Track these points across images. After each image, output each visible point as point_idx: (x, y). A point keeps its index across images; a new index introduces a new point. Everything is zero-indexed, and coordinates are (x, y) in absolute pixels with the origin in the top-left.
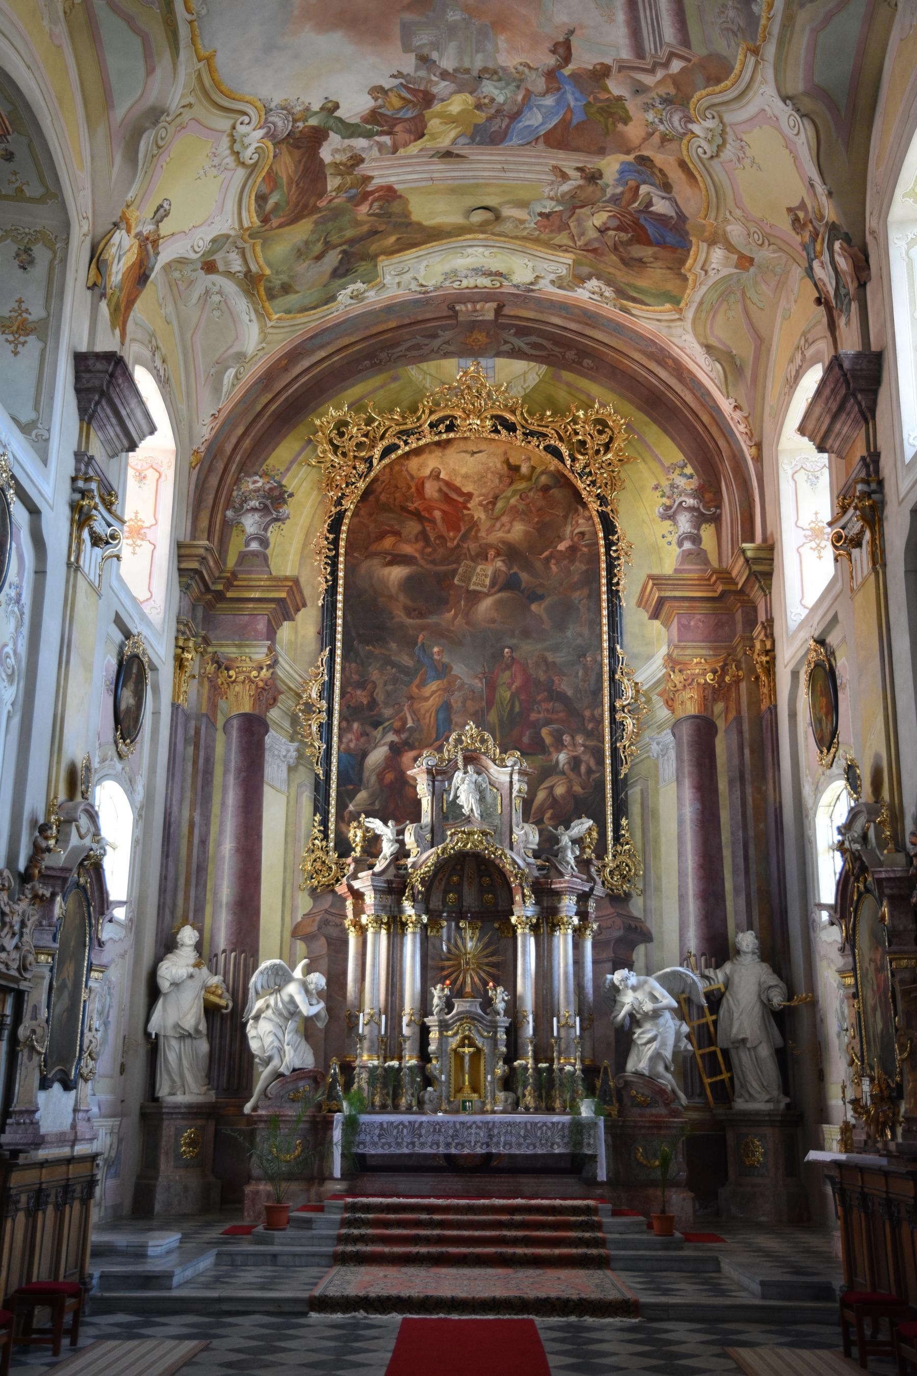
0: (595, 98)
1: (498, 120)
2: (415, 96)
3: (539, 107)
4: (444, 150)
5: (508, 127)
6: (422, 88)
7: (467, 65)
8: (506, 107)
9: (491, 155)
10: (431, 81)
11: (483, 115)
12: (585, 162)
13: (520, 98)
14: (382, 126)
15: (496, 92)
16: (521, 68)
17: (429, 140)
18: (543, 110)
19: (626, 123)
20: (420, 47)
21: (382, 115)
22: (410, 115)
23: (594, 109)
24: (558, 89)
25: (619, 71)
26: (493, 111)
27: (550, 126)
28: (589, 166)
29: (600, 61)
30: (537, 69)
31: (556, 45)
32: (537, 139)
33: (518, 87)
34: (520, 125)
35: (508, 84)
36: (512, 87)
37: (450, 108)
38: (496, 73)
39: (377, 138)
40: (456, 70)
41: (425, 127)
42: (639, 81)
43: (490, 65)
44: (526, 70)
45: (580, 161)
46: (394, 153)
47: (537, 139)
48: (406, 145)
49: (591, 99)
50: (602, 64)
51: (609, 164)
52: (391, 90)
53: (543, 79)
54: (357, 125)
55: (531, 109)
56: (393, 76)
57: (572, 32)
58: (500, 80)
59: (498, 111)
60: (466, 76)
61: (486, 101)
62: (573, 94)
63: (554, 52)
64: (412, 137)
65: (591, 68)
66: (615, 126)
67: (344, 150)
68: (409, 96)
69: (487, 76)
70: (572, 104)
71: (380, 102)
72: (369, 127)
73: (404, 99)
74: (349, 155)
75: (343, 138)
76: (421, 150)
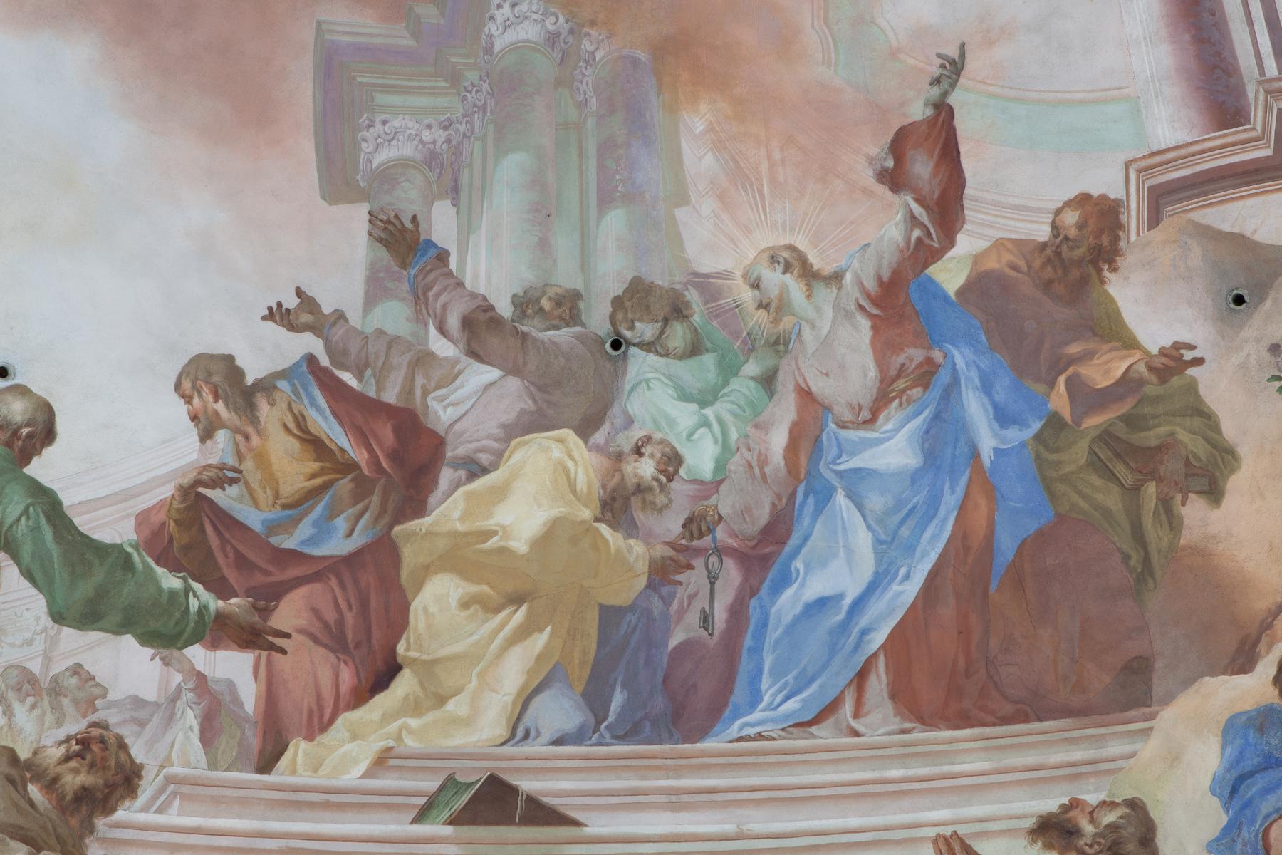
0: (1075, 386)
1: (695, 579)
2: (362, 437)
3: (855, 481)
4: (474, 774)
5: (738, 612)
6: (390, 396)
7: (566, 276)
8: (725, 503)
9: (677, 801)
10: (424, 359)
11: (638, 552)
12: (1075, 773)
13: (778, 440)
14: (222, 589)
15: (685, 415)
16: (774, 278)
17: (414, 707)
18: (876, 502)
19: (1214, 494)
20: (388, 176)
21: (226, 521)
22: (337, 545)
23: (1079, 453)
24: (926, 375)
25: (1155, 219)
26: (672, 525)
27: (907, 590)
28: (1092, 798)
29: (1070, 194)
30: (837, 277)
31: (900, 144)
32: (861, 676)
33: (768, 381)
34: (787, 604)
35: (728, 370)
36: (743, 387)
37: (504, 515)
38: (678, 310)
39: (197, 654)
40: (525, 304)
41: (398, 621)
42: (1239, 241)
43: (659, 276)
44: (795, 288)
45: (1040, 777)
46: (266, 766)
47: (861, 676)
48: (318, 724)
49: (1059, 400)
50: (1083, 200)
51: (1174, 758)
52: (266, 386)
53: (865, 324)
54: (116, 557)
55: (824, 497)
56: (277, 314)
57: (954, 68)
58: (694, 349)
59: (696, 525)
60: (563, 335)
61: (646, 468)
62: (987, 387)
63: (894, 179)
64: (347, 677)
65: (1042, 232)
66: (1174, 523)
67: (56, 689)
68: (338, 436)
69: (646, 330)
70: (988, 441)
71: (221, 447)
72: (171, 581)
73: (315, 445)
74: (75, 726)
75: (58, 617)
76: (382, 761)
